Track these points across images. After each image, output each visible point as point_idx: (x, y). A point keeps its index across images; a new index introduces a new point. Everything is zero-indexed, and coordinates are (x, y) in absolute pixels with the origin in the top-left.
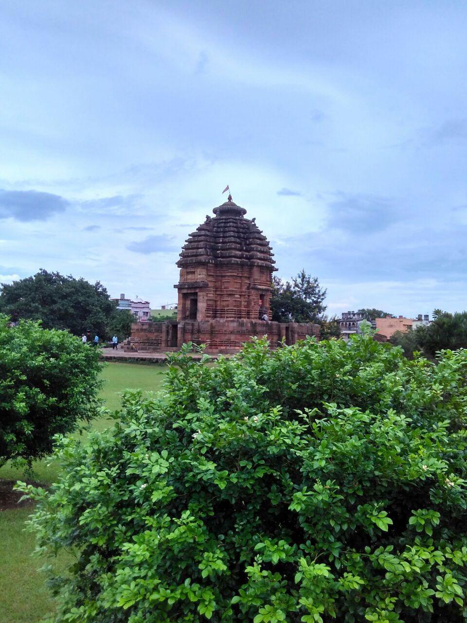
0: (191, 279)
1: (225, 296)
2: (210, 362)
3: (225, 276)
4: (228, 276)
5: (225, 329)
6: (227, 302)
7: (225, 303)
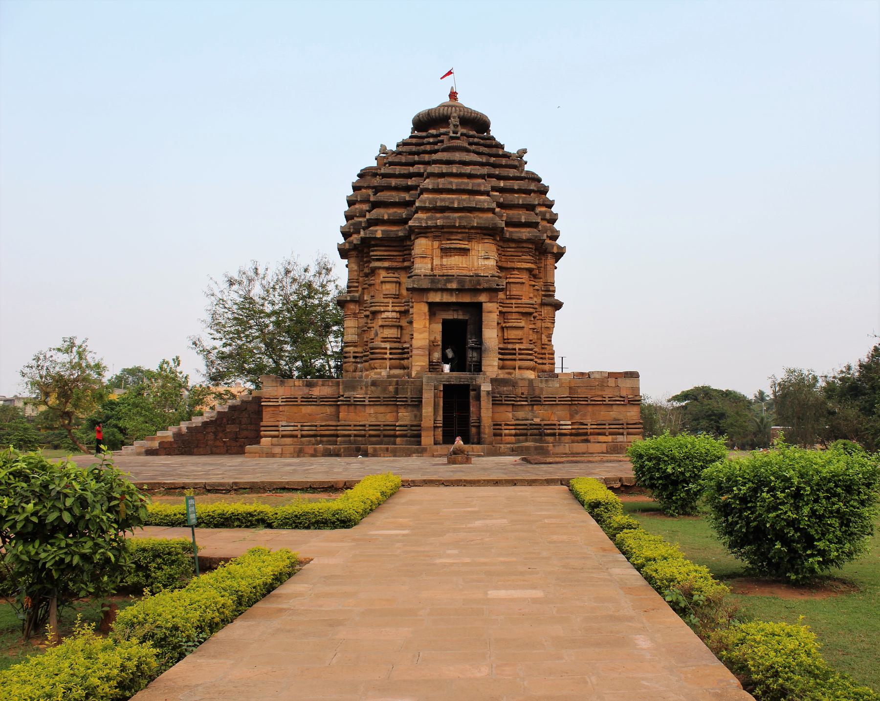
0: (459, 268)
1: (514, 316)
2: (407, 481)
3: (514, 269)
4: (519, 269)
5: (608, 393)
7: (512, 334)
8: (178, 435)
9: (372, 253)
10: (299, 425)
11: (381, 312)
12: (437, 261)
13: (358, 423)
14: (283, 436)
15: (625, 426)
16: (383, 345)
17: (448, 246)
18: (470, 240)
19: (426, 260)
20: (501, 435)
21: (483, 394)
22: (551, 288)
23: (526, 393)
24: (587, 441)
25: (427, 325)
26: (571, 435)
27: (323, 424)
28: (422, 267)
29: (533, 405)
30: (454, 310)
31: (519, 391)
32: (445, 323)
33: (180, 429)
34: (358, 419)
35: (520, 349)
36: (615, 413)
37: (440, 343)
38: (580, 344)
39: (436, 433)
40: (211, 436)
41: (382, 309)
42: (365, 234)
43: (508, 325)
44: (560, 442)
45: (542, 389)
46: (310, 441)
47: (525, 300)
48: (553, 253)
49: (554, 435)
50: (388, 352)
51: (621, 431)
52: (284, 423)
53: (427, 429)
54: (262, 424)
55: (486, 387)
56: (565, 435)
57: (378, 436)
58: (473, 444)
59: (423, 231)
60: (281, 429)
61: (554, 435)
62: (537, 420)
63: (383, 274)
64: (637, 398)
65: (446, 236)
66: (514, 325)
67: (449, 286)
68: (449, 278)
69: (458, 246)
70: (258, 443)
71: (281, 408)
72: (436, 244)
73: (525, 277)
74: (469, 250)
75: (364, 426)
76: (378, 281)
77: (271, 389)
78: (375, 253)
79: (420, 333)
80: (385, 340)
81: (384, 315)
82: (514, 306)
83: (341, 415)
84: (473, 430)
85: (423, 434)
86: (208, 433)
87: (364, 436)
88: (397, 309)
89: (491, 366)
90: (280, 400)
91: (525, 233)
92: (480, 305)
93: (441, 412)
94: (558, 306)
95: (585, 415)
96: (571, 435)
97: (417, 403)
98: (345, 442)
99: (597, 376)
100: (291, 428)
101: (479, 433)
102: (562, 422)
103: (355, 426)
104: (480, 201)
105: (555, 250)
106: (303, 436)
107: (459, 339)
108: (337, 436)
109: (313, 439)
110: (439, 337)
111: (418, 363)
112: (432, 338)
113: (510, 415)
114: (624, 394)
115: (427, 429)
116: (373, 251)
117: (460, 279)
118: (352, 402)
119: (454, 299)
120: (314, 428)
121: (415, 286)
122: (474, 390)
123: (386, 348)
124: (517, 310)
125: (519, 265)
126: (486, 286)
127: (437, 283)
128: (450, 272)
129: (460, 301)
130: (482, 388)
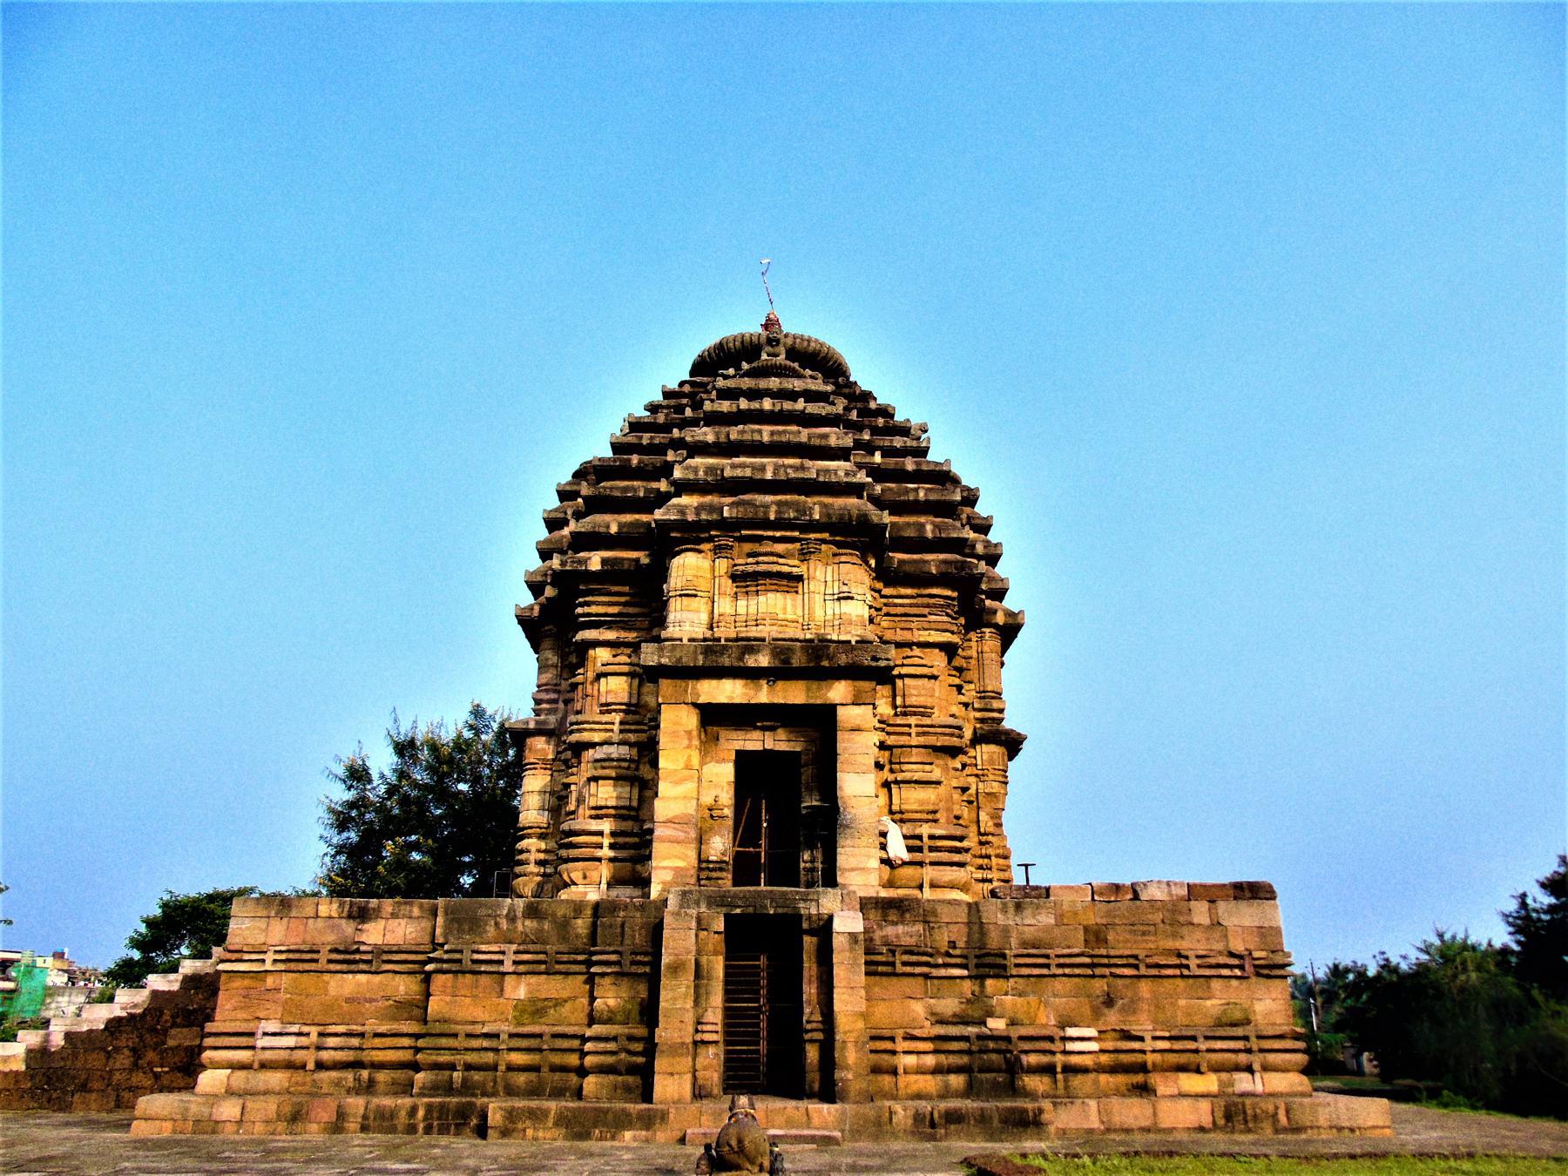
0: (775, 620)
6: (928, 795)
8: (39, 1056)
9: (579, 610)
10: (314, 1030)
11: (593, 745)
12: (724, 606)
13: (478, 1029)
14: (264, 1066)
15: (1254, 1044)
16: (594, 825)
17: (750, 569)
18: (804, 556)
19: (694, 602)
20: (894, 1072)
21: (838, 942)
22: (996, 704)
23: (961, 944)
24: (1145, 1090)
25: (695, 761)
26: (1100, 1069)
27: (383, 1029)
28: (686, 621)
29: (981, 978)
30: (764, 729)
31: (942, 938)
32: (744, 760)
33: (47, 1039)
34: (479, 1014)
35: (931, 837)
36: (1218, 1000)
37: (729, 812)
38: (1059, 834)
39: (700, 1062)
40: (123, 1060)
41: (597, 737)
42: (563, 564)
43: (900, 777)
44: (1070, 1096)
45: (1006, 931)
46: (338, 1084)
47: (939, 717)
48: (996, 626)
49: (1049, 1070)
50: (606, 841)
51: (1243, 1058)
52: (273, 1026)
53: (675, 1050)
54: (210, 1027)
55: (848, 923)
56: (1084, 1070)
57: (534, 1069)
58: (811, 1096)
59: (691, 534)
60: (260, 1043)
61: (1049, 1070)
62: (997, 1024)
63: (603, 654)
64: (1279, 959)
65: (748, 547)
66: (916, 776)
67: (750, 661)
68: (749, 645)
69: (776, 568)
70: (190, 1087)
71: (270, 981)
72: (723, 565)
73: (938, 660)
74: (800, 578)
75: (497, 1036)
76: (591, 675)
77: (248, 924)
78: (587, 610)
79: (678, 783)
80: (599, 813)
81: (600, 753)
82: (913, 731)
83: (435, 1005)
84: (812, 1053)
85: (660, 1064)
86: (117, 1050)
87: (495, 1068)
88: (632, 737)
89: (861, 870)
90: (269, 957)
91: (933, 561)
92: (830, 710)
93: (717, 998)
94: (1013, 744)
95: (1131, 1009)
96: (1100, 1069)
97: (647, 970)
98: (434, 1089)
99: (1158, 894)
100: (290, 1041)
101: (828, 1062)
102: (1071, 1032)
103: (469, 1036)
104: (827, 471)
105: (1000, 619)
106: (320, 1066)
107: (787, 809)
108: (416, 1067)
109: (349, 1076)
110: (727, 797)
111: (669, 864)
112: (707, 800)
113: (918, 1008)
114: (1238, 946)
115: (675, 1050)
116: (582, 605)
117: (781, 649)
118: (468, 965)
119: (763, 694)
120: (355, 1042)
121: (664, 661)
122: (811, 932)
123: (601, 833)
124: (922, 740)
125: (924, 636)
126: (843, 660)
127: (717, 658)
128: (753, 632)
129: (779, 699)
130: (837, 925)
